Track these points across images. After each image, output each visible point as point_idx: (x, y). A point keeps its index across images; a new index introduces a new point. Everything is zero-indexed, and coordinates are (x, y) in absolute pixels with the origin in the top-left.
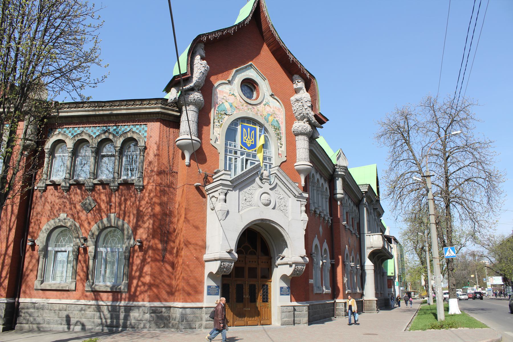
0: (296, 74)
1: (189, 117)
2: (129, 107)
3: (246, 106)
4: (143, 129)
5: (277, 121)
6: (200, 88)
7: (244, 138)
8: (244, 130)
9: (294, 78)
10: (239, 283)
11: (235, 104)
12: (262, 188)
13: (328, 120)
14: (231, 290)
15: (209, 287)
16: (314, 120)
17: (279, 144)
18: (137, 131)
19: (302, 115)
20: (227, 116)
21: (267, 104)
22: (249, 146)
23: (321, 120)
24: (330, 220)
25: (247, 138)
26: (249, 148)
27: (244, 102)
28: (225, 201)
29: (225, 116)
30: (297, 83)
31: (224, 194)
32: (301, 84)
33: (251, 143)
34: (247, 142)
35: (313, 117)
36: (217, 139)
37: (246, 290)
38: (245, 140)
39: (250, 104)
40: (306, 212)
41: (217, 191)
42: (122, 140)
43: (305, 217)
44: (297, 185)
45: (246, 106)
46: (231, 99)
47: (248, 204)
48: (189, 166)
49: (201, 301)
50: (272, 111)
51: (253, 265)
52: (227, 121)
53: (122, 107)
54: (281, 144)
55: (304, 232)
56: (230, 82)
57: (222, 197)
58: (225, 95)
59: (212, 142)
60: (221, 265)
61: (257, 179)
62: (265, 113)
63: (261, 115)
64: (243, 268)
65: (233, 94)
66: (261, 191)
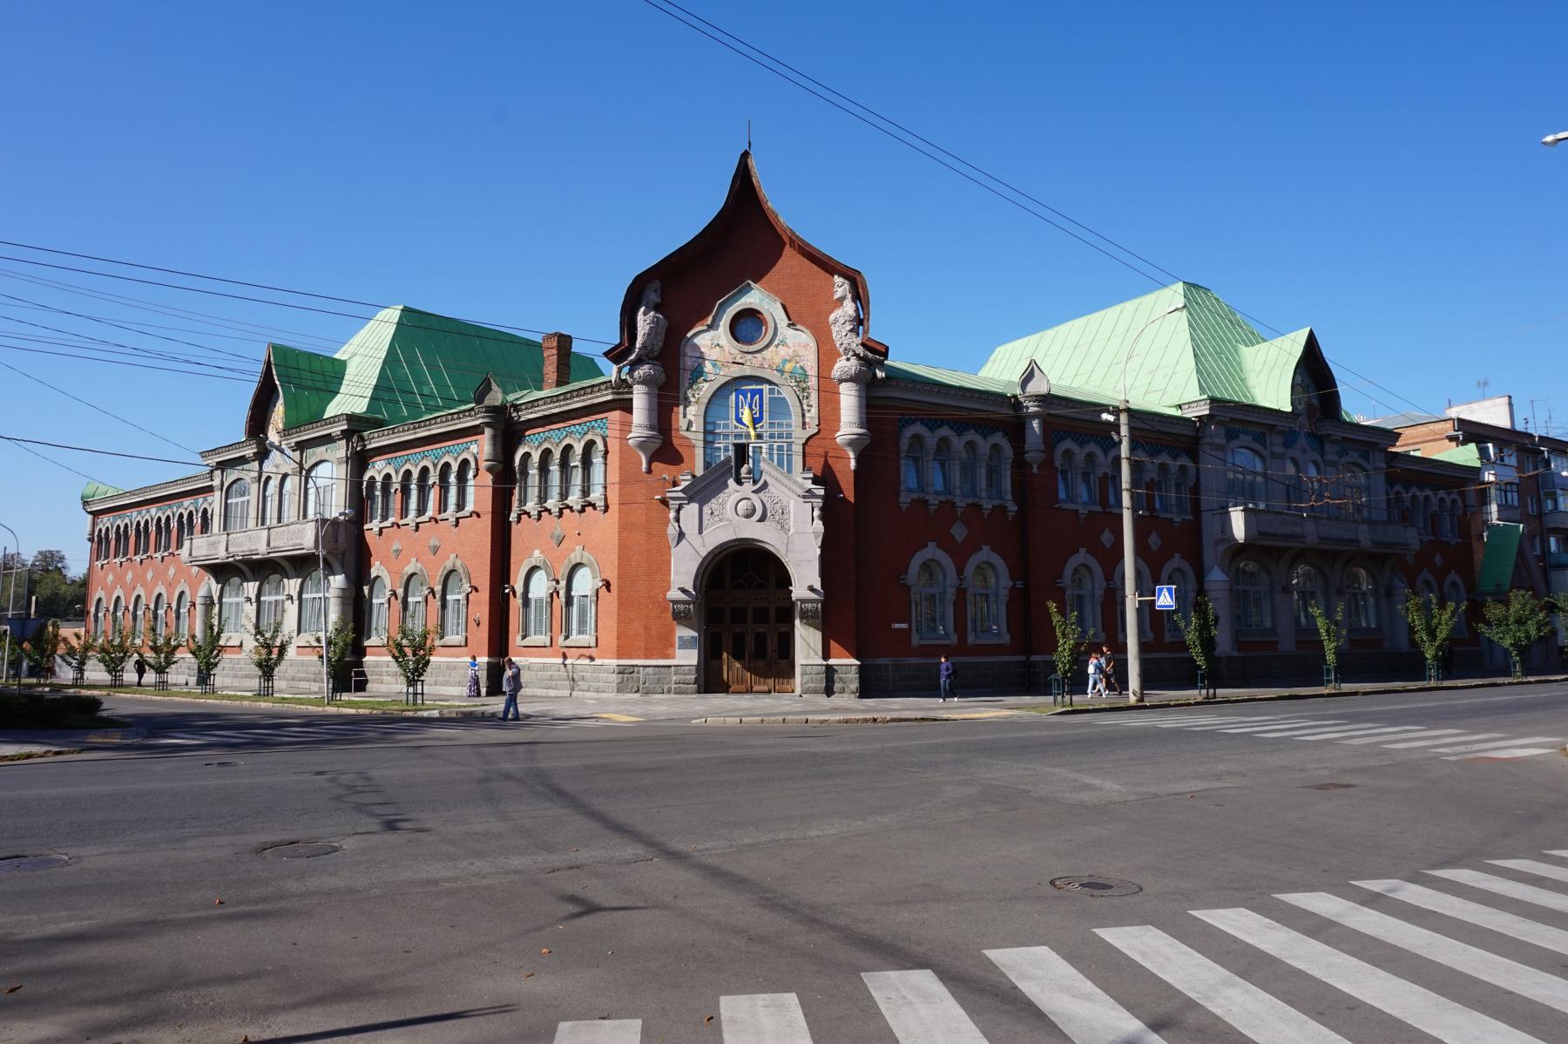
16: (861, 351)
21: (783, 343)
24: (1012, 508)
28: (677, 520)
36: (690, 424)
37: (750, 642)
40: (823, 518)
42: (583, 443)
43: (819, 526)
48: (649, 471)
50: (790, 352)
52: (705, 390)
55: (818, 551)
56: (710, 327)
61: (731, 482)
62: (778, 360)
66: (738, 496)
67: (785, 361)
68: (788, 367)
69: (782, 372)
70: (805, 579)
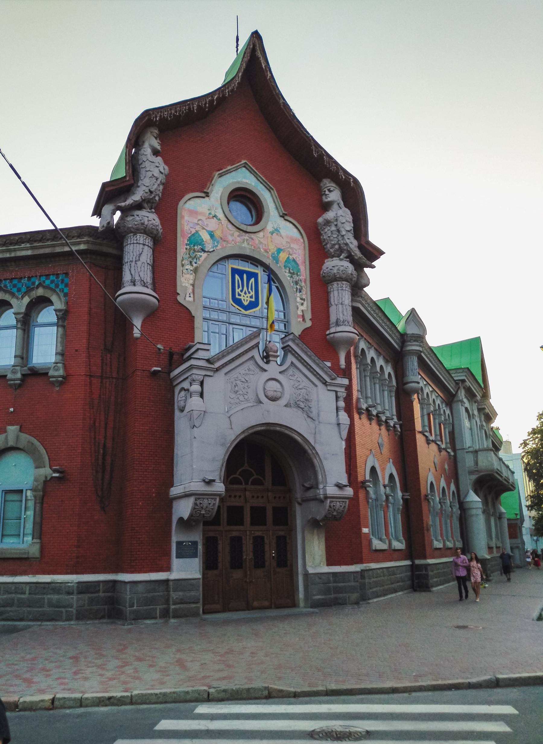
0: (326, 177)
1: (138, 257)
2: (36, 244)
3: (239, 236)
4: (62, 281)
5: (294, 260)
6: (154, 205)
7: (238, 291)
8: (237, 277)
9: (322, 185)
10: (234, 534)
11: (218, 234)
12: (265, 371)
13: (382, 253)
14: (220, 547)
15: (179, 544)
16: (358, 253)
17: (298, 299)
18: (53, 286)
19: (337, 247)
20: (206, 254)
21: (276, 231)
22: (246, 303)
23: (372, 254)
25: (242, 291)
26: (246, 308)
27: (234, 229)
28: (202, 395)
29: (202, 254)
30: (327, 192)
31: (198, 383)
32: (334, 195)
33: (249, 299)
34: (242, 297)
35: (357, 249)
38: (239, 295)
39: (246, 232)
41: (187, 378)
42: (26, 300)
44: (329, 364)
45: (239, 236)
46: (212, 225)
47: (241, 398)
49: (168, 568)
50: (284, 243)
51: (258, 503)
53: (23, 245)
54: (301, 299)
55: (344, 443)
57: (196, 387)
58: (200, 217)
59: (180, 299)
60: (196, 504)
62: (272, 248)
63: (266, 251)
64: (241, 509)
65: (215, 216)
66: (265, 376)
67: (279, 250)
68: (283, 256)
69: (276, 259)
70: (333, 473)
